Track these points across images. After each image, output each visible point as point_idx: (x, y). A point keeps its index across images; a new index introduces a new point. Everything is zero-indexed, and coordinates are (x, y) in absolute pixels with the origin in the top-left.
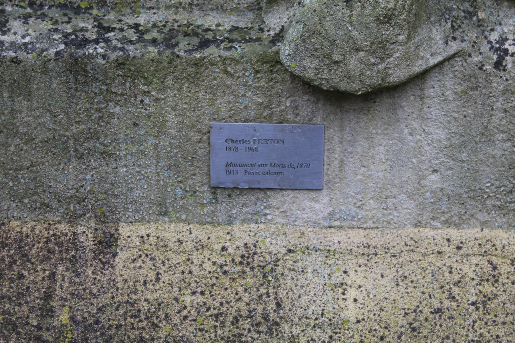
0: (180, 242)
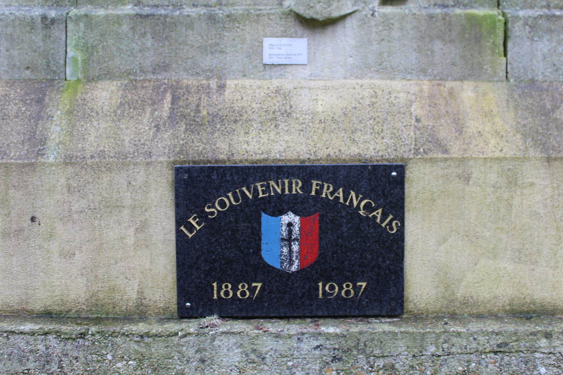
0: (251, 86)
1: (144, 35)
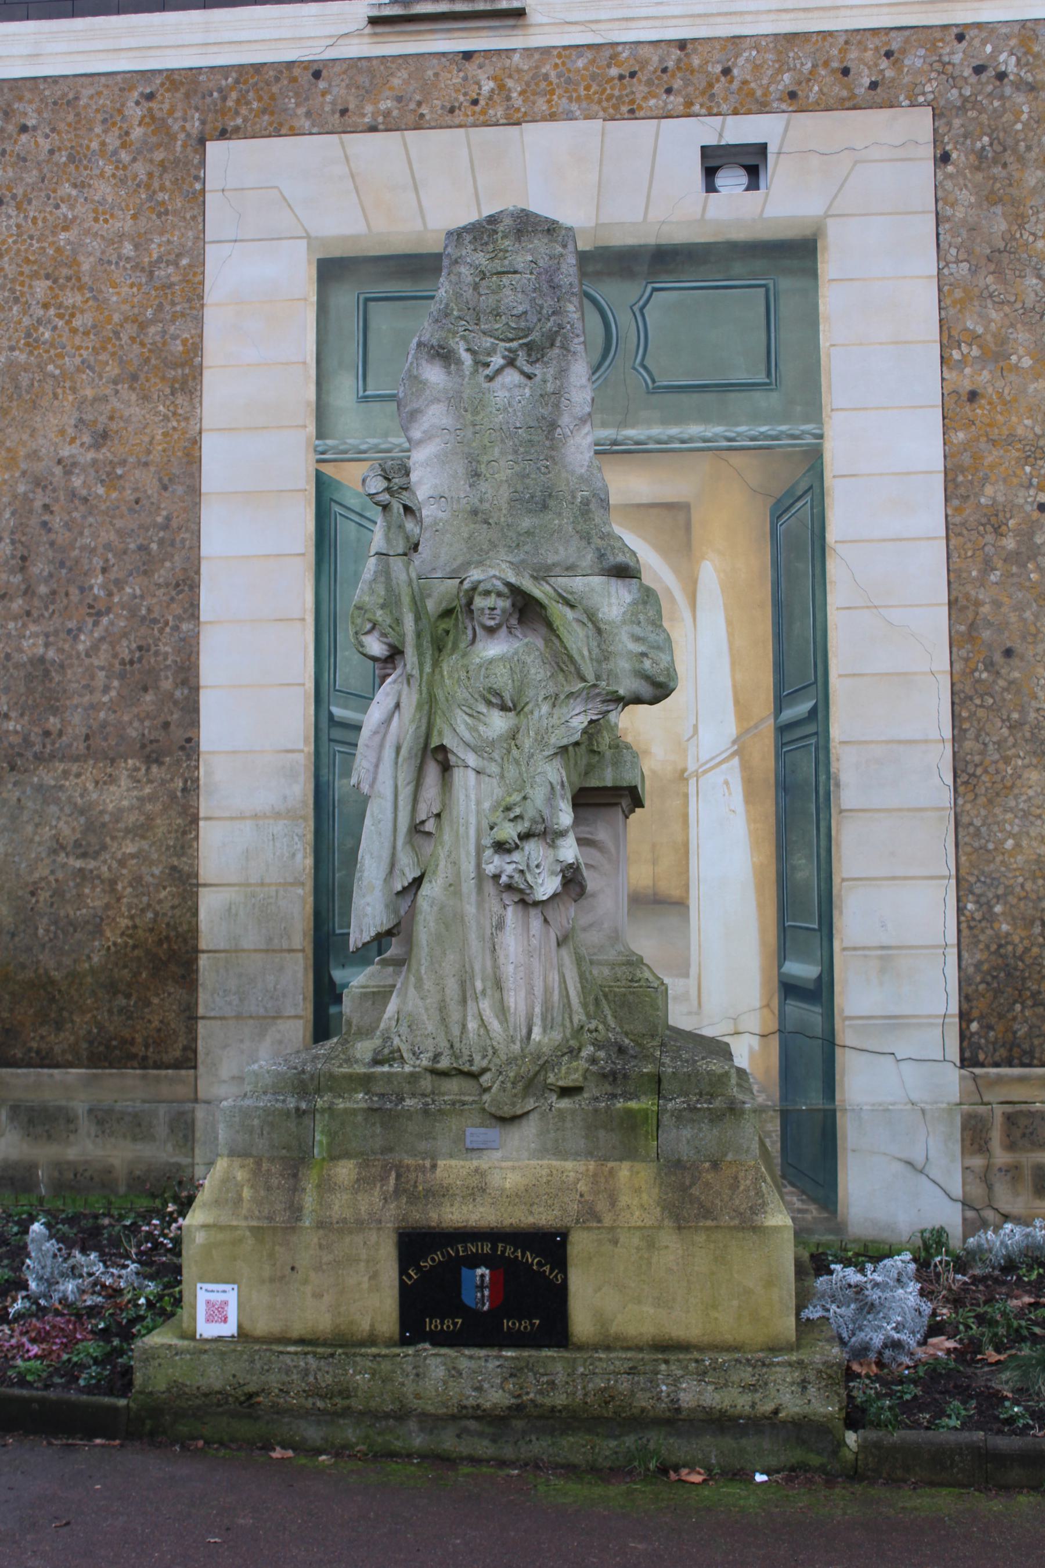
1: (374, 1124)
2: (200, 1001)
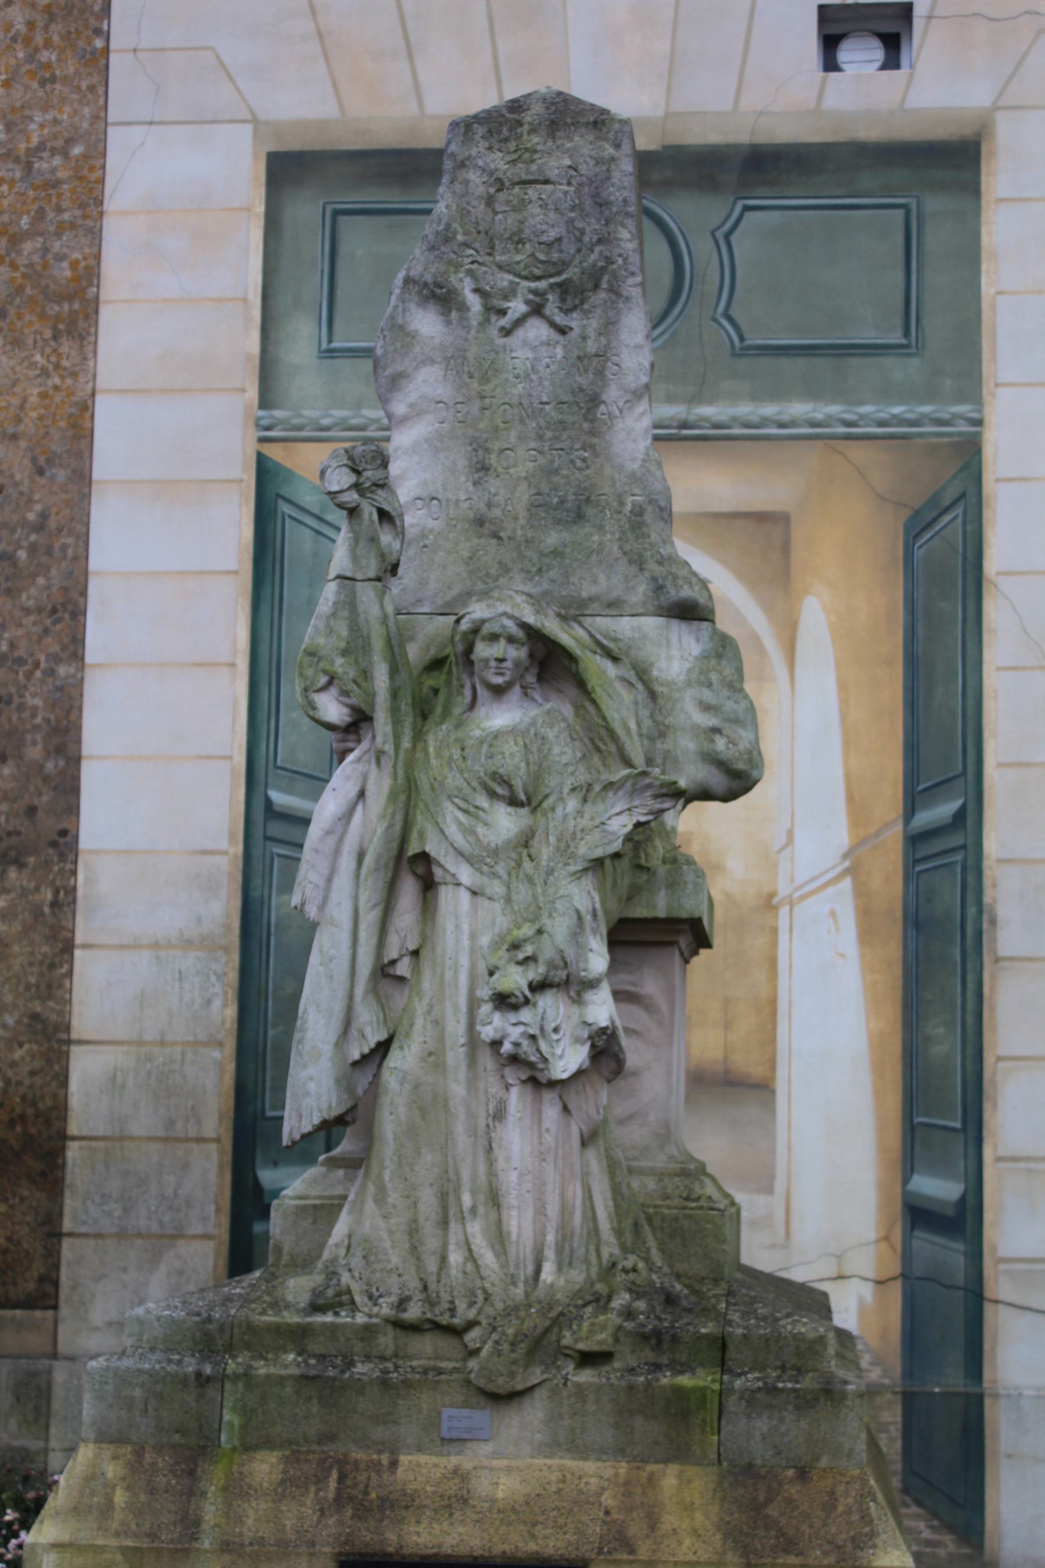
1: (309, 1399)
2: (67, 1210)
